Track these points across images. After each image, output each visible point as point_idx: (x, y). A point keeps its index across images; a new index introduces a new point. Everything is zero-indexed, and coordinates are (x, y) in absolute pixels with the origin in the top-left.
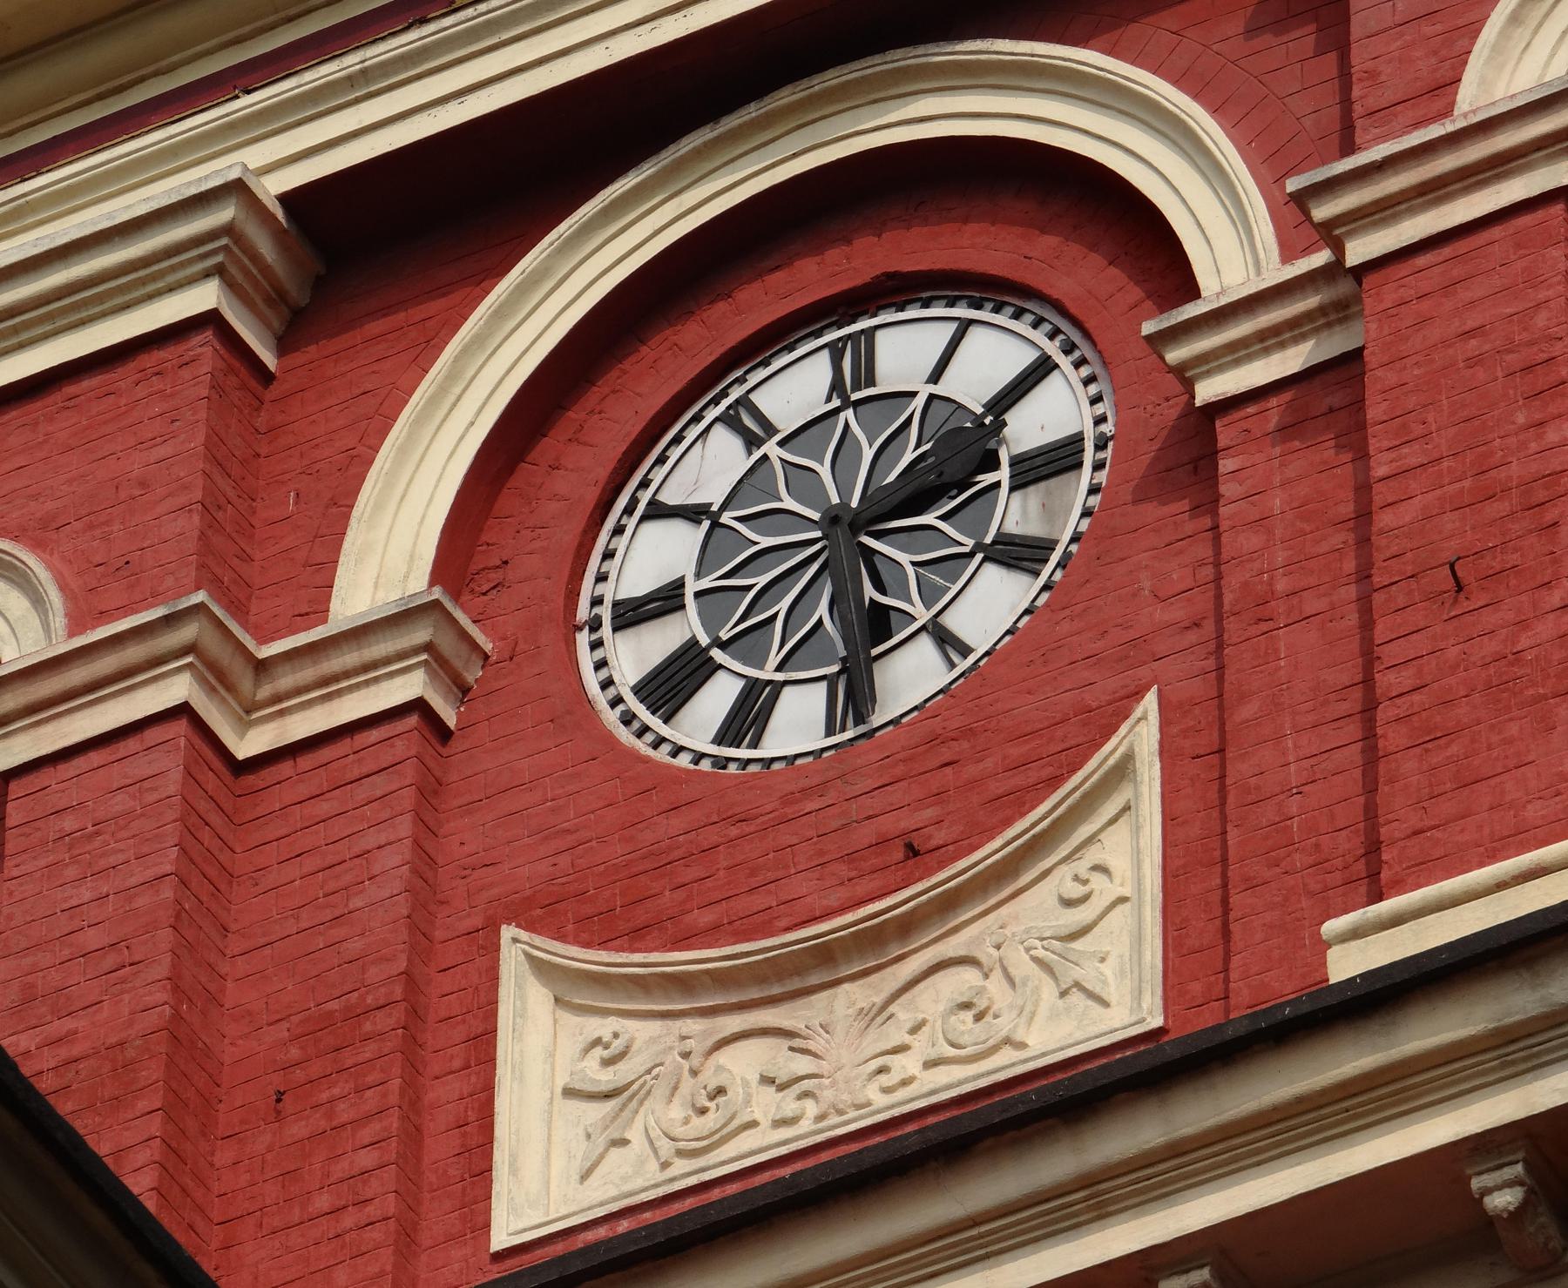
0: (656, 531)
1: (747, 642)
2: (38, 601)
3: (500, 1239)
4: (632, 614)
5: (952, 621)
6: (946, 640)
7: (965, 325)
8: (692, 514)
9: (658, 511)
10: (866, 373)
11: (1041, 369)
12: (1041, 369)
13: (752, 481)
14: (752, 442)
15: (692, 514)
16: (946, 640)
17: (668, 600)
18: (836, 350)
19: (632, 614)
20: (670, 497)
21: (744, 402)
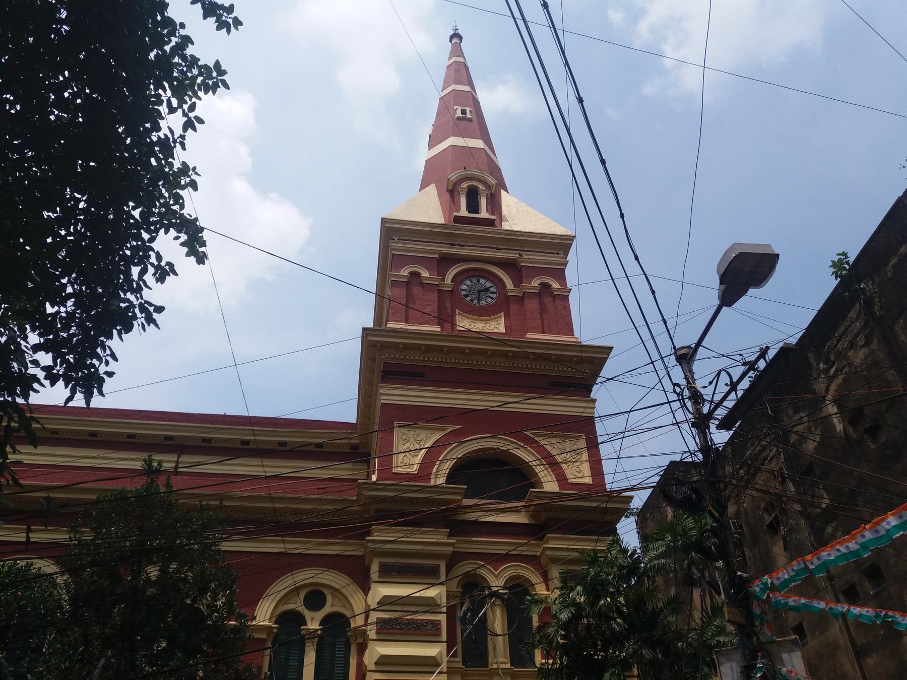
0: (464, 285)
4: (463, 290)
6: (486, 302)
8: (467, 286)
9: (464, 284)
12: (492, 287)
15: (467, 286)
16: (486, 302)
19: (463, 290)
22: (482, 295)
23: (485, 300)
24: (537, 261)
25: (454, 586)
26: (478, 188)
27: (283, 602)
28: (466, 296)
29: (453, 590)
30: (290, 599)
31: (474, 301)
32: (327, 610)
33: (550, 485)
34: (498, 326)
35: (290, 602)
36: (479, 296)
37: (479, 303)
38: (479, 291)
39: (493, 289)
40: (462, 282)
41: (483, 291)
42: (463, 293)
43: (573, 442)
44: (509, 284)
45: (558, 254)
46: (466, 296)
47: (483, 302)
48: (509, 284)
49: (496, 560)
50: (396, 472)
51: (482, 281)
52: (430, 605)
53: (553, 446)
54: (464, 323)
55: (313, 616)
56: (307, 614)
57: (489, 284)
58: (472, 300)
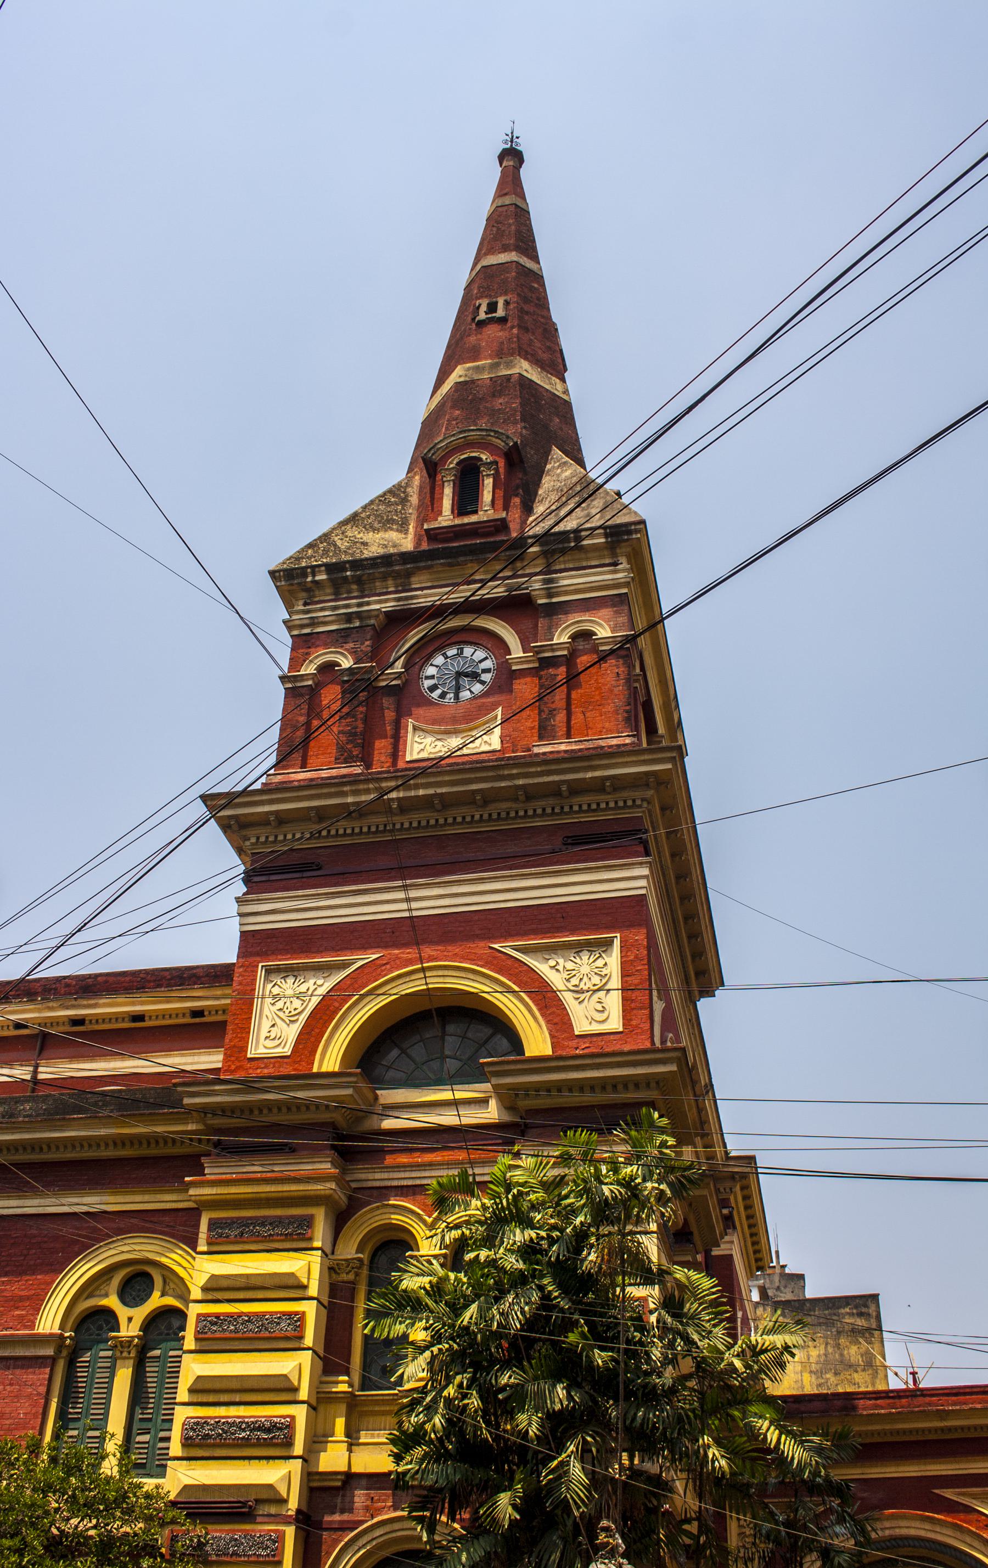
4: (427, 678)
5: (472, 689)
6: (471, 692)
7: (476, 650)
8: (437, 666)
9: (432, 665)
10: (462, 653)
11: (486, 658)
12: (486, 658)
14: (446, 659)
15: (437, 666)
16: (471, 692)
17: (432, 677)
18: (458, 649)
19: (427, 678)
20: (434, 663)
21: (445, 653)
22: (465, 681)
23: (469, 689)
25: (349, 1250)
26: (480, 459)
27: (85, 1295)
28: (433, 688)
30: (97, 1288)
31: (448, 696)
32: (156, 1301)
35: (98, 1293)
36: (457, 682)
37: (457, 697)
38: (459, 674)
39: (488, 664)
41: (467, 675)
42: (428, 683)
43: (597, 952)
44: (517, 652)
46: (433, 688)
47: (465, 695)
48: (517, 652)
50: (253, 1056)
51: (468, 651)
55: (130, 1315)
56: (123, 1312)
57: (480, 654)
58: (443, 695)
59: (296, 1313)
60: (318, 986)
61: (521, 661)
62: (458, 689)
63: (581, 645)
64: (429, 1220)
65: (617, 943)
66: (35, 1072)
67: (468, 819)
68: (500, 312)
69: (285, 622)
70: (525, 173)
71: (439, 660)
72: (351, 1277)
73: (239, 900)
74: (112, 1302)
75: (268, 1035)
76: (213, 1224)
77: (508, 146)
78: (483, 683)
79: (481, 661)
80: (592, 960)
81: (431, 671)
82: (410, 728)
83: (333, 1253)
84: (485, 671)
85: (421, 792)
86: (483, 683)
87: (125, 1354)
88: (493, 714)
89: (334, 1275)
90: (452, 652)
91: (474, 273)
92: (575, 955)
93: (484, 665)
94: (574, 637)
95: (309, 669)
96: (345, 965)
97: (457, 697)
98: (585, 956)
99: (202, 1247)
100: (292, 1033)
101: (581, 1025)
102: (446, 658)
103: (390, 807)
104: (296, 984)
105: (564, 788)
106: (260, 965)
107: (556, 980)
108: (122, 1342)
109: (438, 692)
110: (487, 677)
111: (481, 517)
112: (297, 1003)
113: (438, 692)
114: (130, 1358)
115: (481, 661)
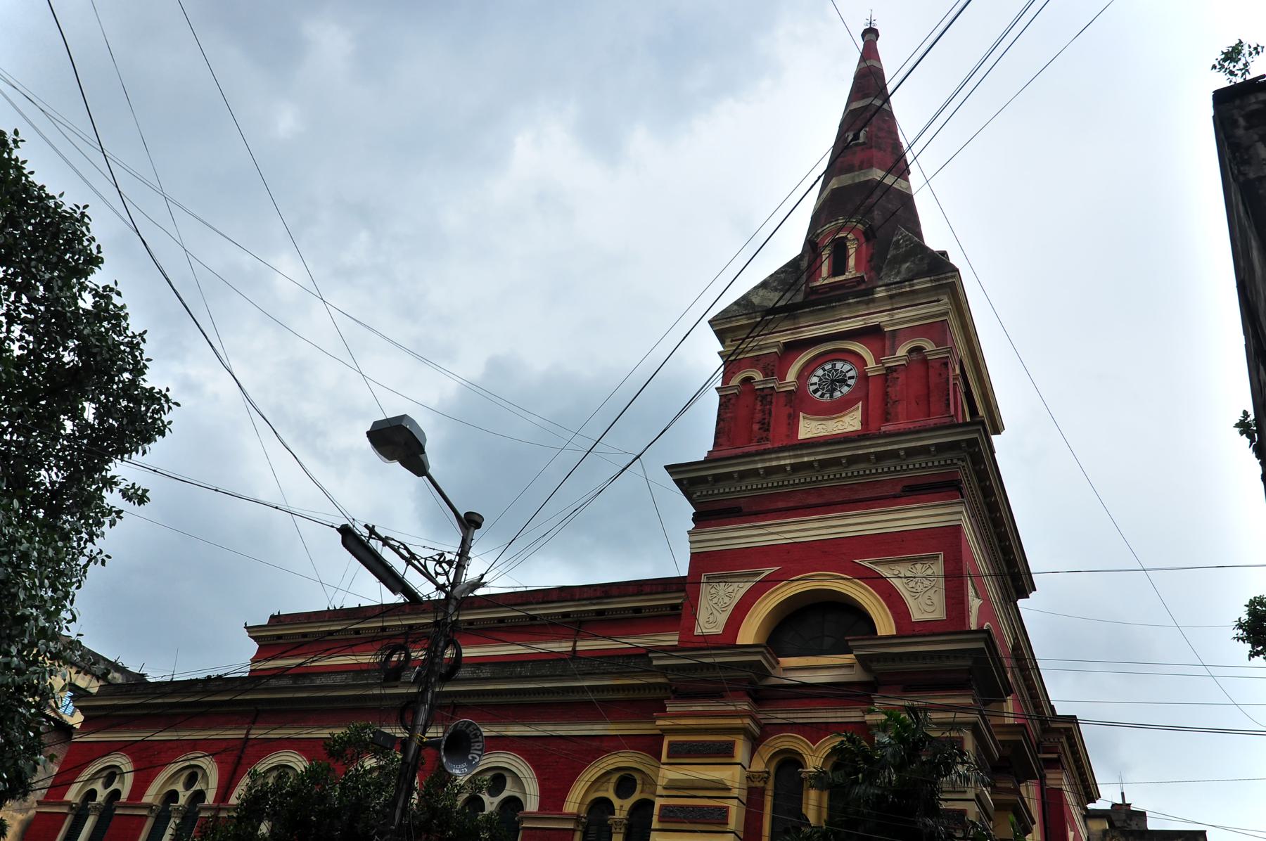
0: (814, 378)
1: (823, 389)
2: (759, 375)
3: (800, 437)
4: (812, 384)
6: (841, 392)
8: (818, 377)
9: (815, 376)
11: (851, 369)
12: (851, 369)
13: (824, 375)
15: (818, 377)
16: (841, 392)
17: (815, 384)
19: (812, 384)
23: (840, 391)
24: (902, 320)
28: (815, 391)
29: (760, 770)
30: (601, 785)
31: (826, 396)
32: (636, 796)
33: (885, 624)
34: (851, 422)
35: (602, 788)
37: (831, 396)
38: (832, 381)
40: (812, 373)
42: (812, 388)
44: (871, 363)
45: (938, 301)
46: (815, 391)
47: (837, 394)
48: (871, 363)
49: (815, 732)
51: (839, 365)
52: (721, 787)
53: (896, 574)
54: (809, 428)
55: (621, 804)
56: (617, 802)
57: (847, 367)
58: (822, 395)
59: (724, 807)
60: (739, 589)
61: (873, 370)
62: (834, 390)
63: (914, 356)
64: (814, 747)
65: (941, 558)
66: (574, 646)
67: (838, 476)
68: (861, 140)
69: (719, 353)
70: (880, 44)
71: (820, 372)
72: (761, 784)
73: (689, 532)
74: (611, 795)
75: (708, 620)
76: (671, 744)
77: (868, 27)
78: (849, 386)
79: (847, 372)
80: (923, 570)
81: (815, 380)
82: (801, 418)
83: (750, 767)
84: (850, 378)
85: (806, 459)
86: (849, 386)
87: (618, 830)
88: (856, 406)
89: (750, 782)
90: (828, 367)
91: (846, 112)
92: (912, 567)
93: (849, 374)
94: (911, 351)
95: (735, 381)
96: (759, 574)
97: (831, 396)
98: (919, 566)
99: (664, 758)
100: (723, 618)
101: (916, 616)
102: (825, 370)
103: (786, 469)
104: (726, 587)
105: (902, 453)
106: (703, 574)
107: (897, 583)
108: (616, 822)
109: (819, 393)
110: (851, 382)
111: (848, 276)
112: (726, 600)
113: (819, 393)
114: (621, 833)
115: (847, 372)
